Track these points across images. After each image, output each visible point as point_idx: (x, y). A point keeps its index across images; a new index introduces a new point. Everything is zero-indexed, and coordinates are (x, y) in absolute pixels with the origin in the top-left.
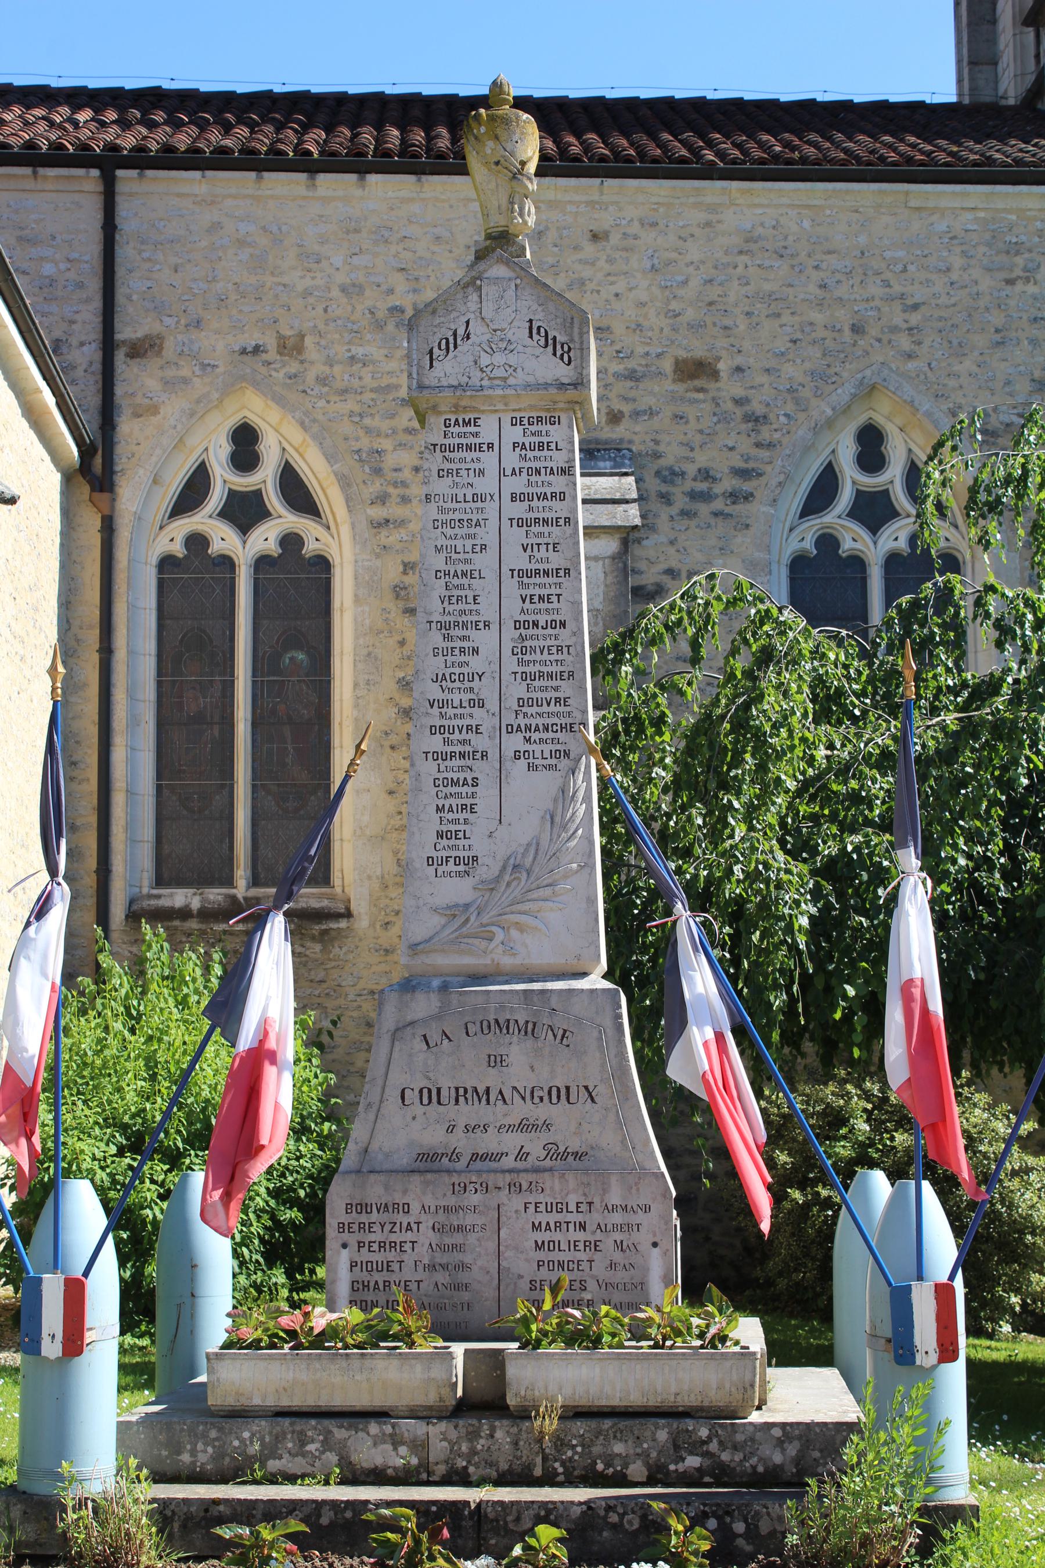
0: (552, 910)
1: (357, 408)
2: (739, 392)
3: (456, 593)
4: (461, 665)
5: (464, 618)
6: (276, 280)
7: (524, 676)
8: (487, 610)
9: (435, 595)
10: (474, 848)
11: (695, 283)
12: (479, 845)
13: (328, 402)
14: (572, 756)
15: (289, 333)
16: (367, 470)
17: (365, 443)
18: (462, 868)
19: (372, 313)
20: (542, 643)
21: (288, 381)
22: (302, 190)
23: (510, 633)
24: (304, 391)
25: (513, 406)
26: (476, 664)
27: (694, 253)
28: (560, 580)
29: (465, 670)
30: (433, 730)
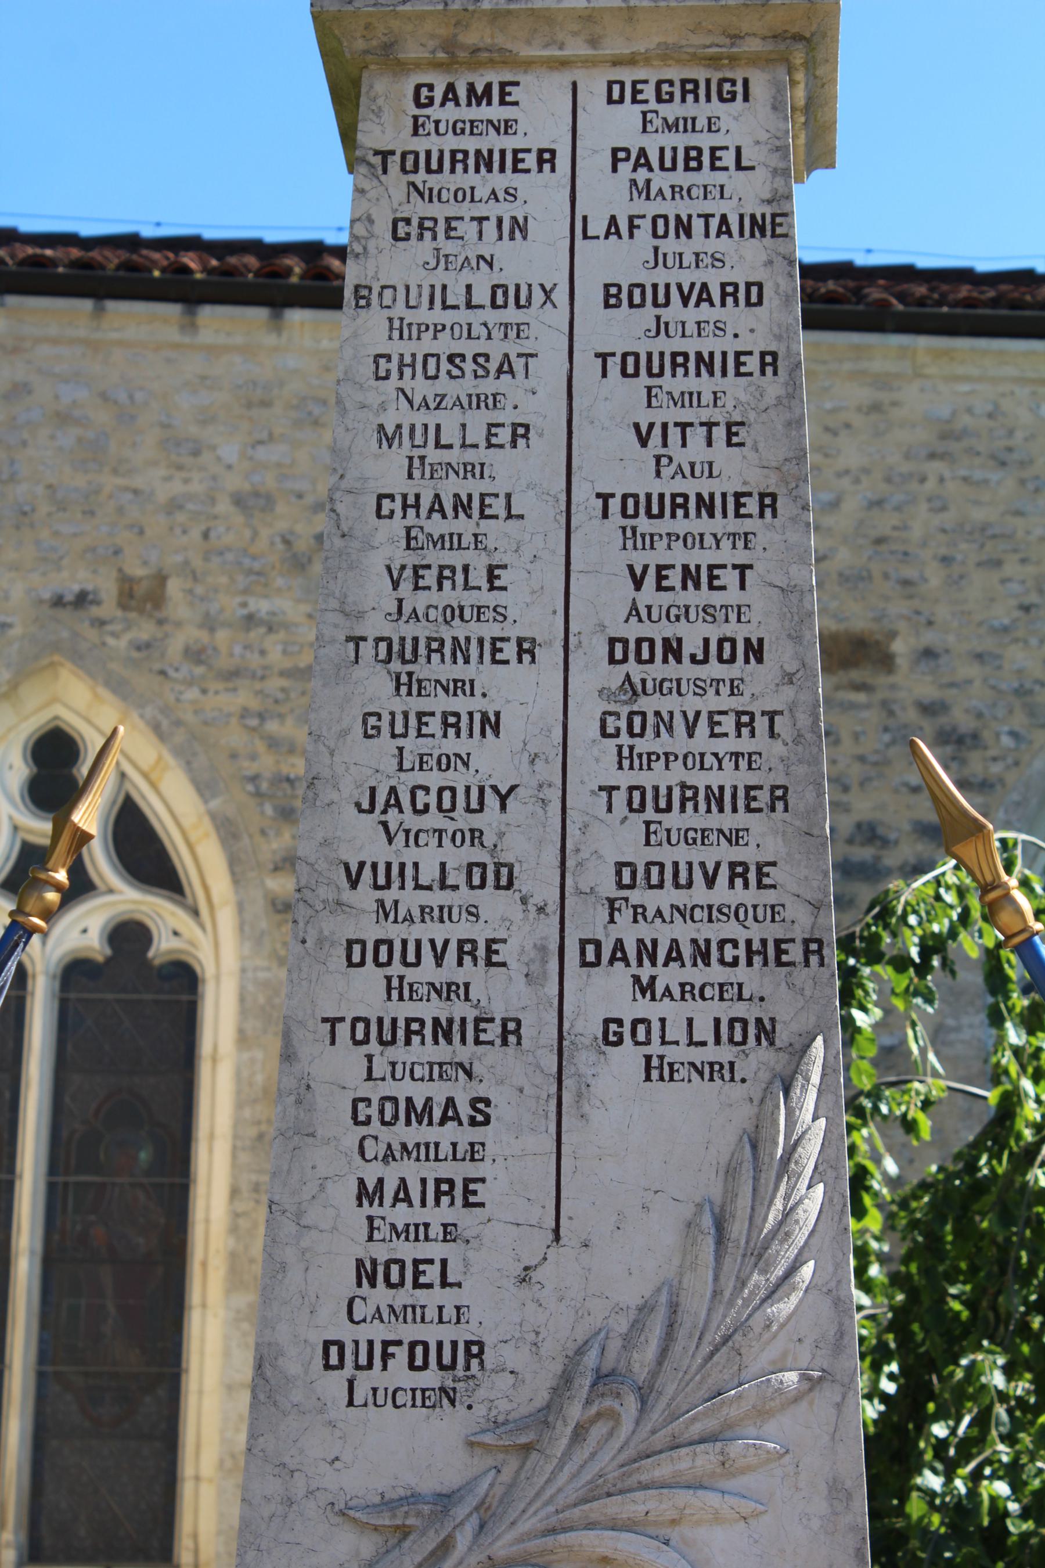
0: (717, 1519)
1: (254, 704)
2: (927, 690)
3: (435, 557)
4: (445, 763)
5: (460, 630)
6: (120, 481)
7: (638, 800)
8: (528, 605)
9: (376, 562)
10: (474, 1315)
11: (851, 505)
12: (487, 1306)
13: (204, 691)
14: (782, 1036)
15: (139, 572)
16: (269, 810)
17: (266, 764)
18: (431, 1378)
19: (287, 542)
20: (692, 703)
21: (135, 654)
22: (172, 334)
23: (593, 674)
24: (163, 673)
25: (615, 46)
26: (491, 761)
27: (851, 454)
28: (747, 525)
29: (458, 778)
30: (356, 957)
